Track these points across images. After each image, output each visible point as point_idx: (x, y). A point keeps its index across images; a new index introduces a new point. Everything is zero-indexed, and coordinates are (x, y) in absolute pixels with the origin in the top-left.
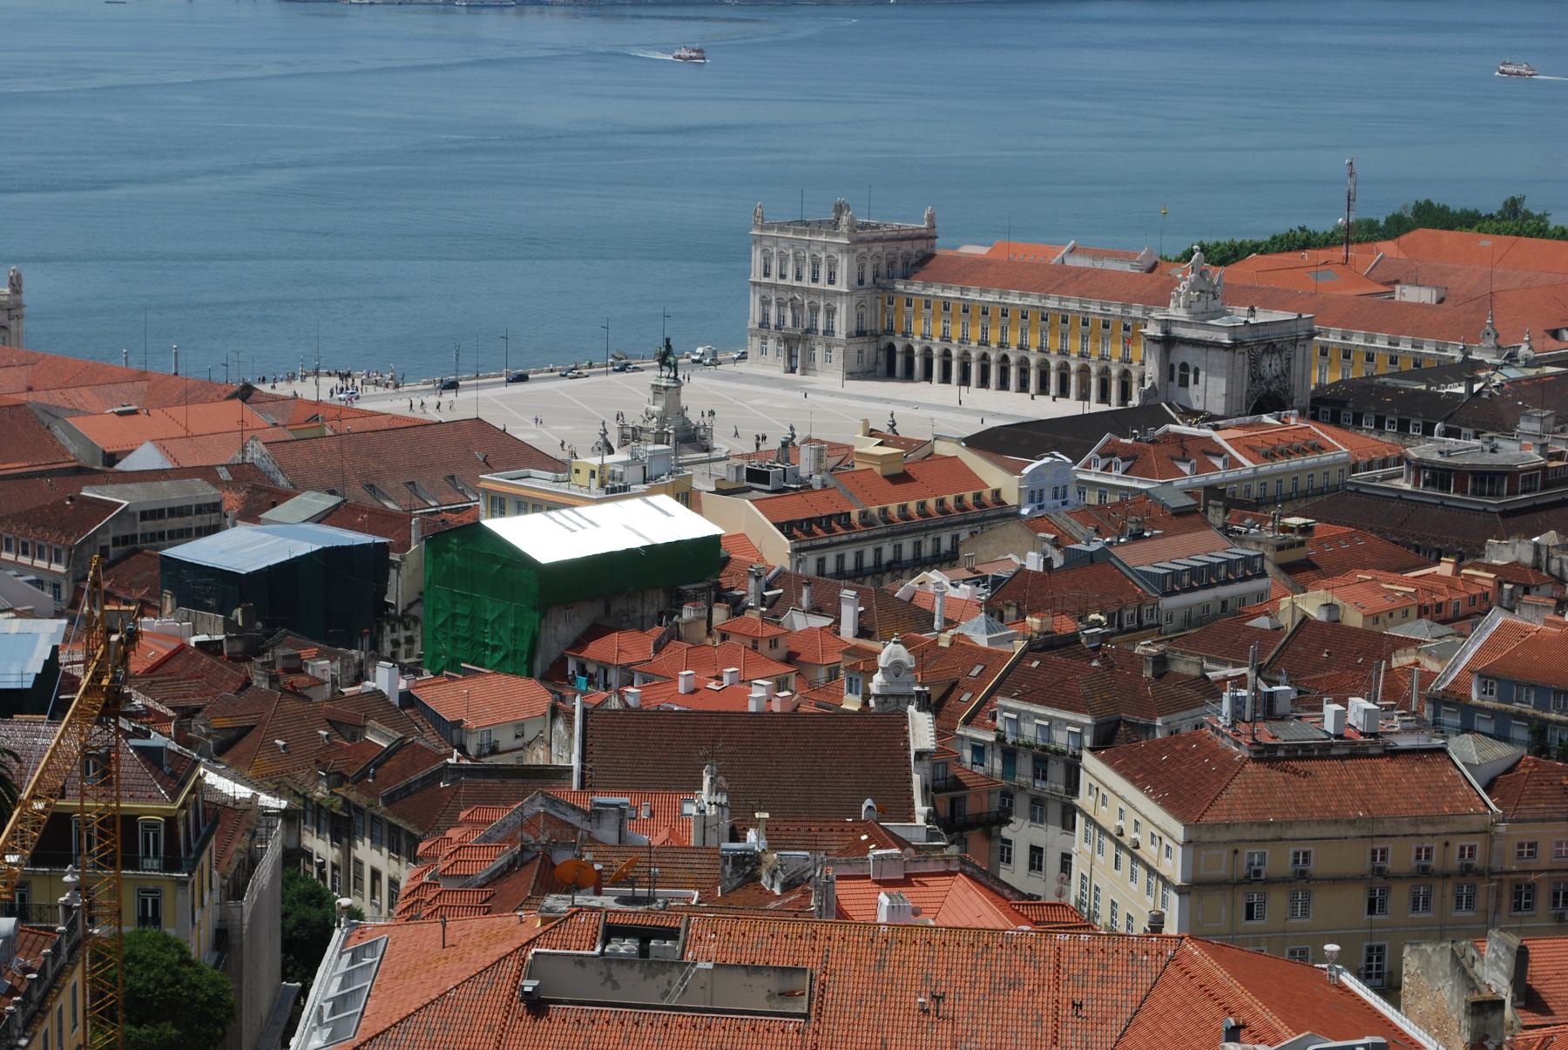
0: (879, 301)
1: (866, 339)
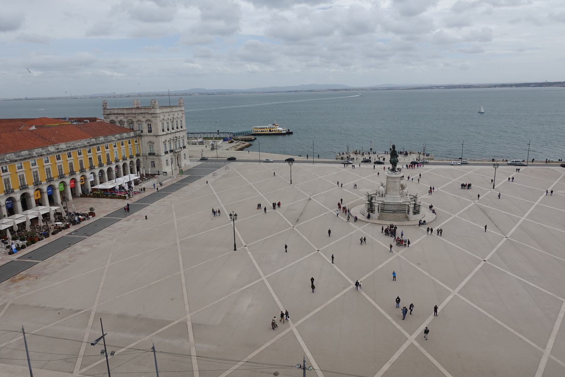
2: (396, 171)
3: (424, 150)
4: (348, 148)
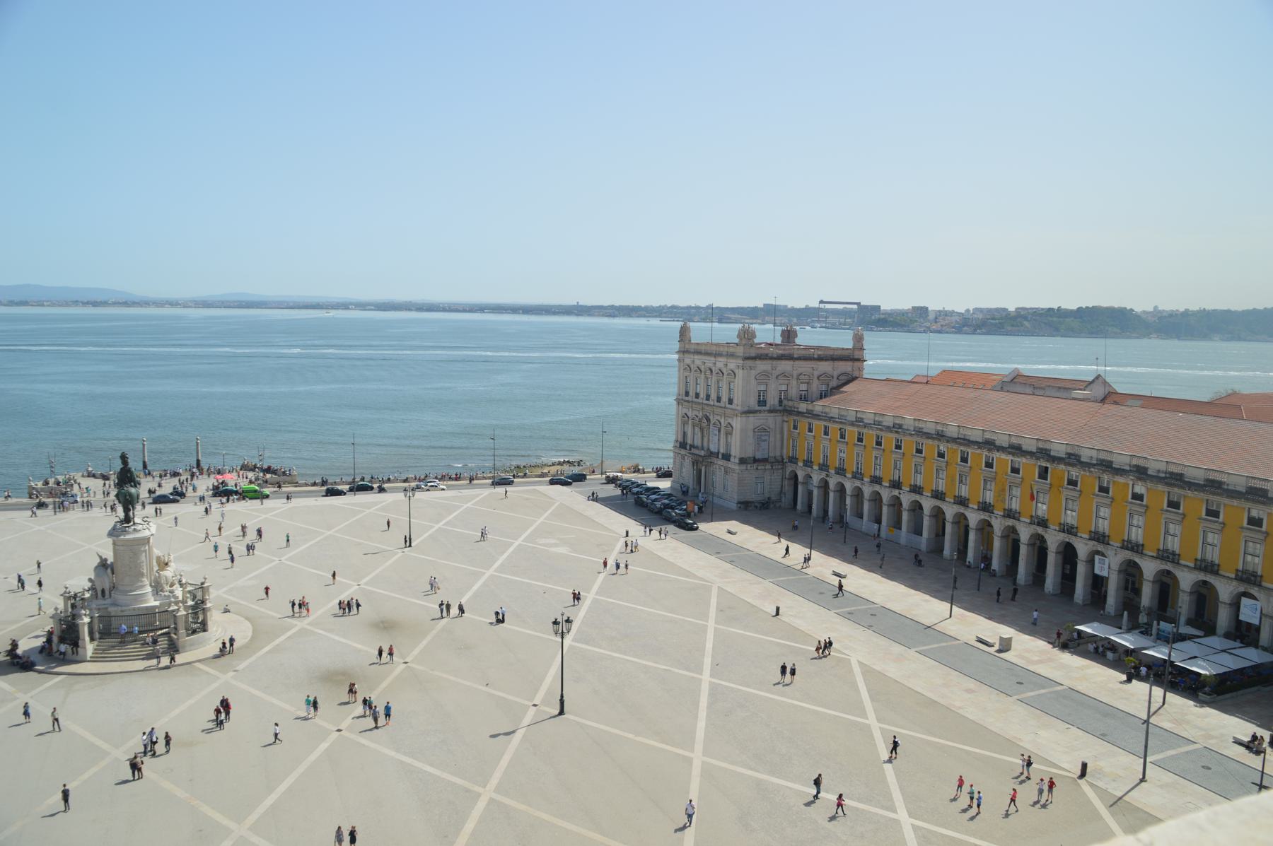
0: (785, 424)
1: (768, 466)
2: (134, 524)
3: (261, 458)
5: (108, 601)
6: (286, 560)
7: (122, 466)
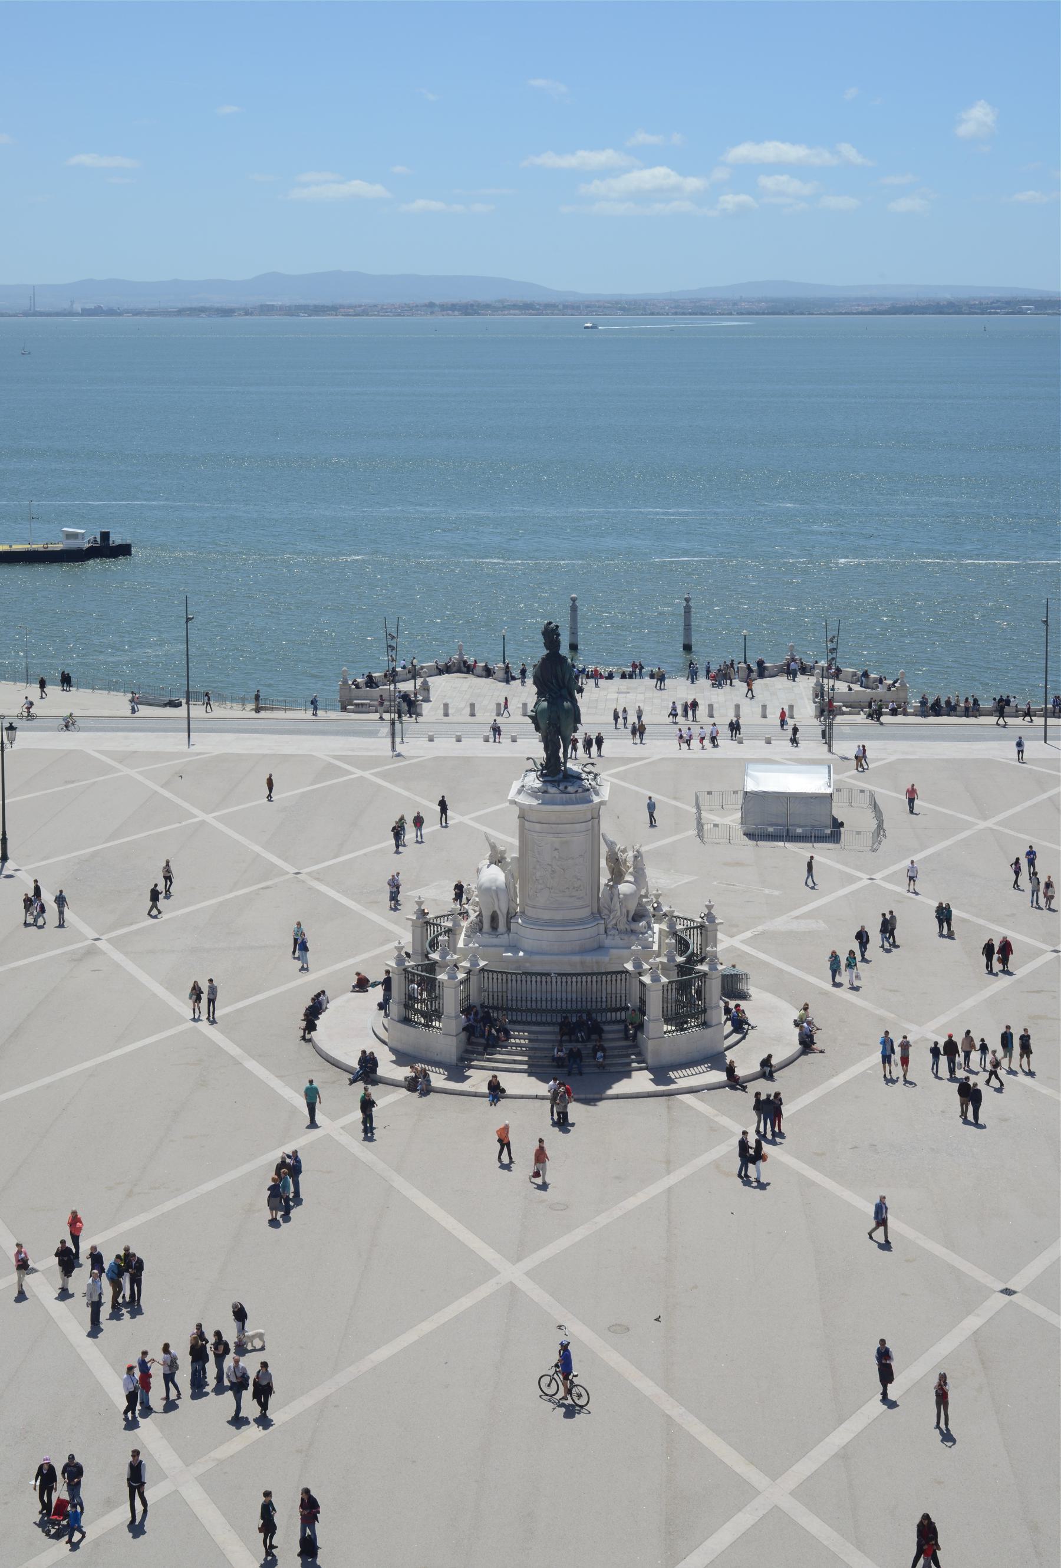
4: (393, 643)
5: (504, 939)
6: (883, 879)
7: (545, 652)
